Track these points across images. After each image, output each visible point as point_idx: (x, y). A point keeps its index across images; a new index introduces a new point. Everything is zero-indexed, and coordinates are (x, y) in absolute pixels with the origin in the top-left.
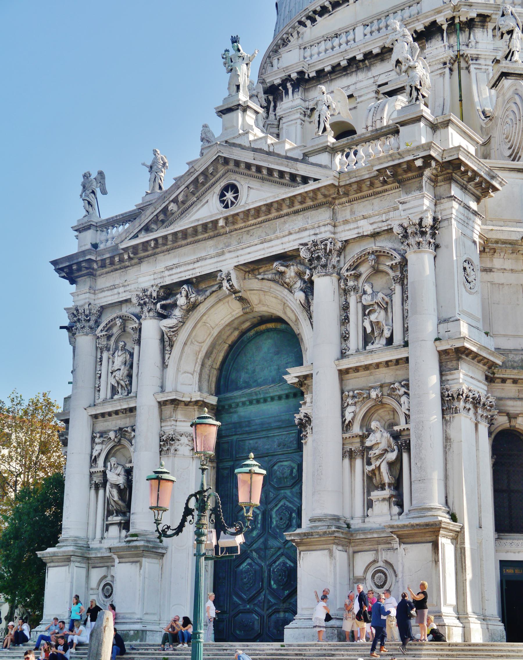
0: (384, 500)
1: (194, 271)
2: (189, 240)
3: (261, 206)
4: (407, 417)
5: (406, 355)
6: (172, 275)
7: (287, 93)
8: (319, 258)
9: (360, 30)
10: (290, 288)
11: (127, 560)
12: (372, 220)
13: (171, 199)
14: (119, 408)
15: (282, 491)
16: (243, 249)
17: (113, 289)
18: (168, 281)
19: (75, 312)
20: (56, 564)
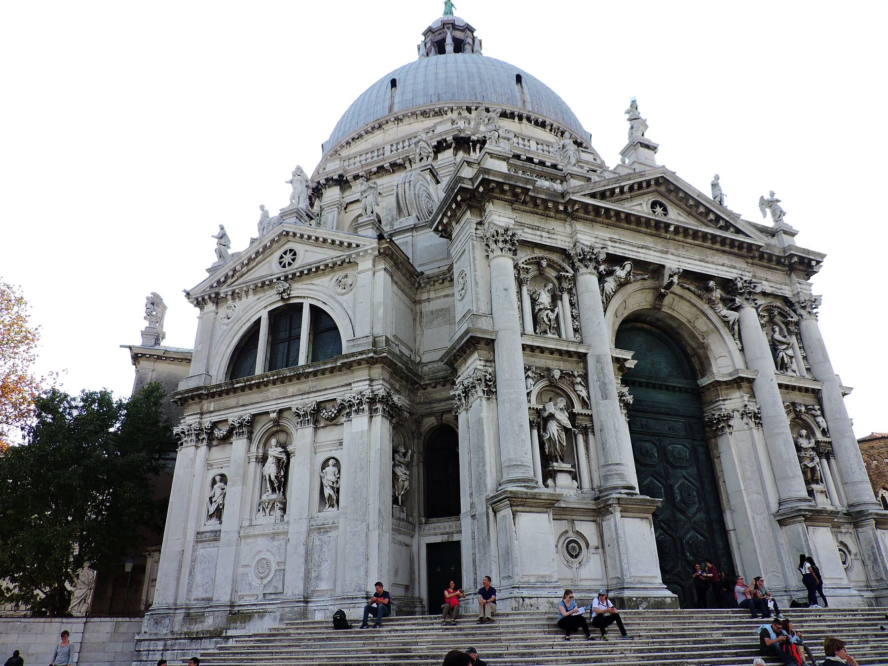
0: (822, 492)
1: (638, 254)
2: (631, 227)
3: (709, 233)
5: (820, 388)
6: (616, 247)
7: (474, 150)
8: (750, 293)
11: (631, 515)
12: (772, 284)
13: (622, 184)
14: (565, 349)
15: (679, 470)
16: (683, 257)
17: (535, 229)
18: (611, 251)
19: (501, 231)
20: (527, 509)
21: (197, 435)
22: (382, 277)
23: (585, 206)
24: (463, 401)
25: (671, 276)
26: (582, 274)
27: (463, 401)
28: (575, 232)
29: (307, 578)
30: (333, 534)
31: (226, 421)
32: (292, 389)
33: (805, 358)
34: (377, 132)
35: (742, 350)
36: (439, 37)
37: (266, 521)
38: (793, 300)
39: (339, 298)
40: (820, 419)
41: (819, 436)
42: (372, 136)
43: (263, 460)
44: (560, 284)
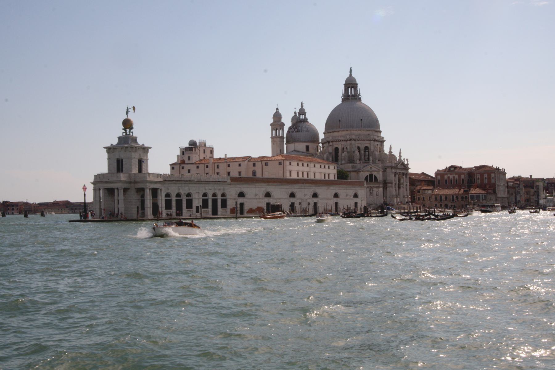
36: (352, 86)
37: (371, 196)
43: (370, 191)
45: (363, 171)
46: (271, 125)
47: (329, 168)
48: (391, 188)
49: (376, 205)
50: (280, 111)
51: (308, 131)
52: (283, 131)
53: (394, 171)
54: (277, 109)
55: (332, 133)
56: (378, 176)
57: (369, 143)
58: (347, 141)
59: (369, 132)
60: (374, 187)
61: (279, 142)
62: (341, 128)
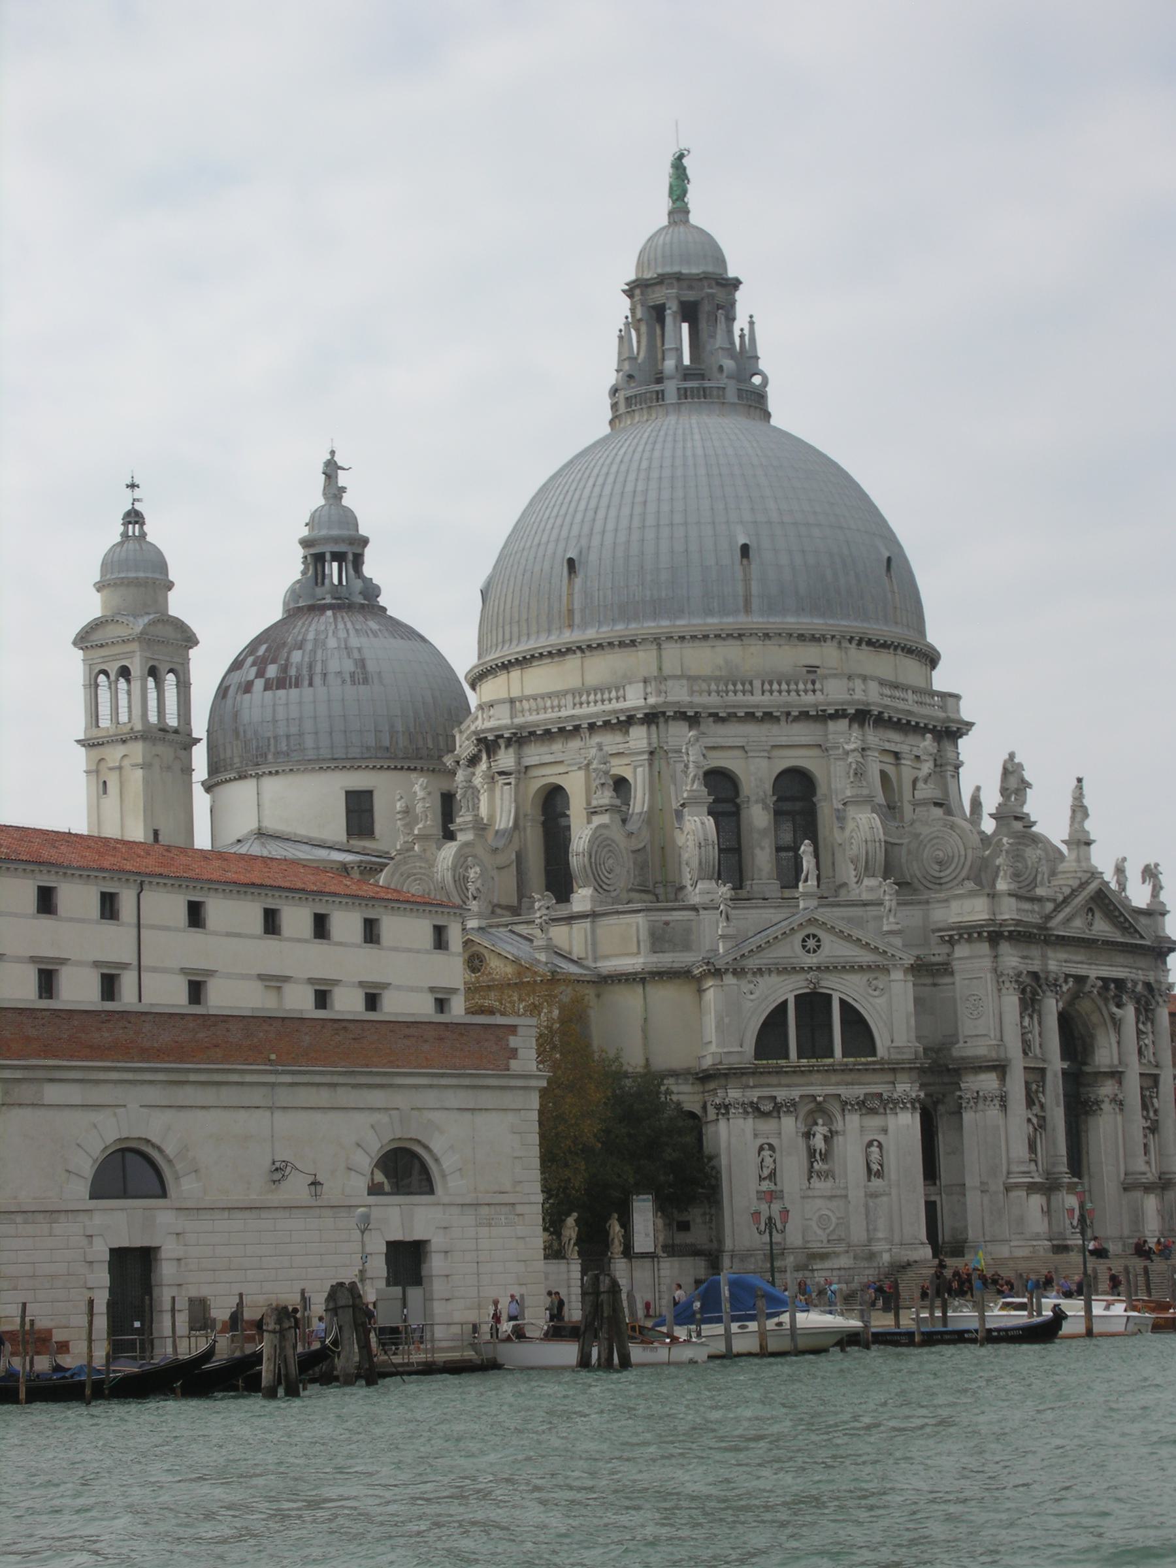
4: (1156, 1111)
9: (910, 692)
10: (1106, 1000)
21: (745, 1109)
22: (910, 984)
23: (1058, 936)
24: (972, 1104)
25: (1092, 986)
26: (1048, 997)
27: (972, 1104)
28: (1044, 957)
29: (868, 1230)
30: (885, 1199)
31: (775, 1098)
32: (834, 1078)
33: (1153, 1042)
34: (730, 642)
35: (1118, 1043)
36: (690, 296)
38: (1154, 985)
39: (871, 999)
40: (1155, 1100)
41: (1151, 1114)
42: (719, 643)
43: (808, 1135)
44: (1033, 1006)
45: (739, 973)
46: (85, 639)
47: (371, 931)
48: (993, 1112)
49: (871, 1256)
50: (155, 532)
51: (361, 675)
52: (184, 687)
53: (1012, 959)
54: (134, 517)
55: (515, 674)
56: (872, 1009)
57: (818, 740)
58: (626, 722)
59: (809, 654)
60: (844, 1104)
61: (139, 773)
62: (585, 625)
